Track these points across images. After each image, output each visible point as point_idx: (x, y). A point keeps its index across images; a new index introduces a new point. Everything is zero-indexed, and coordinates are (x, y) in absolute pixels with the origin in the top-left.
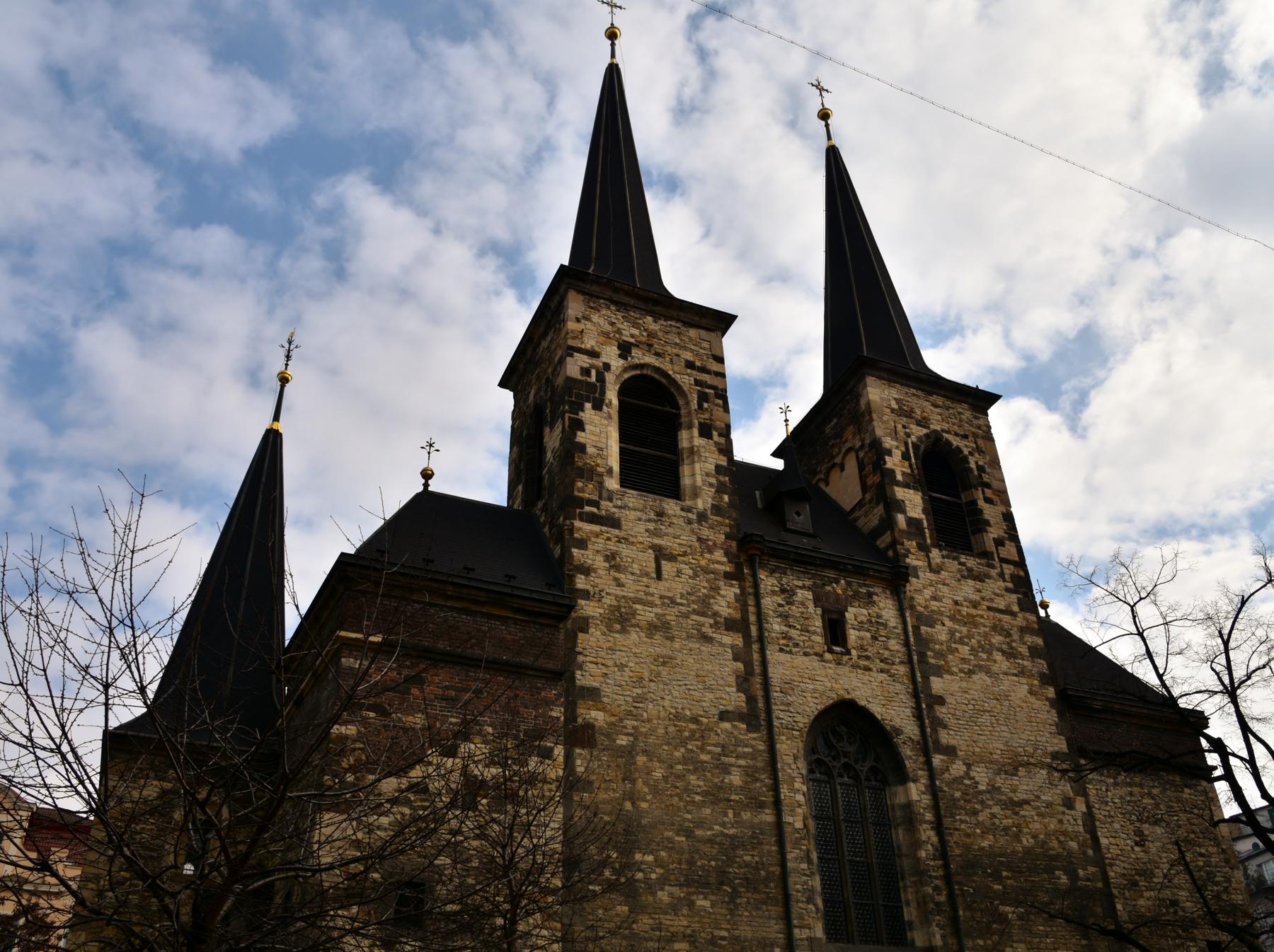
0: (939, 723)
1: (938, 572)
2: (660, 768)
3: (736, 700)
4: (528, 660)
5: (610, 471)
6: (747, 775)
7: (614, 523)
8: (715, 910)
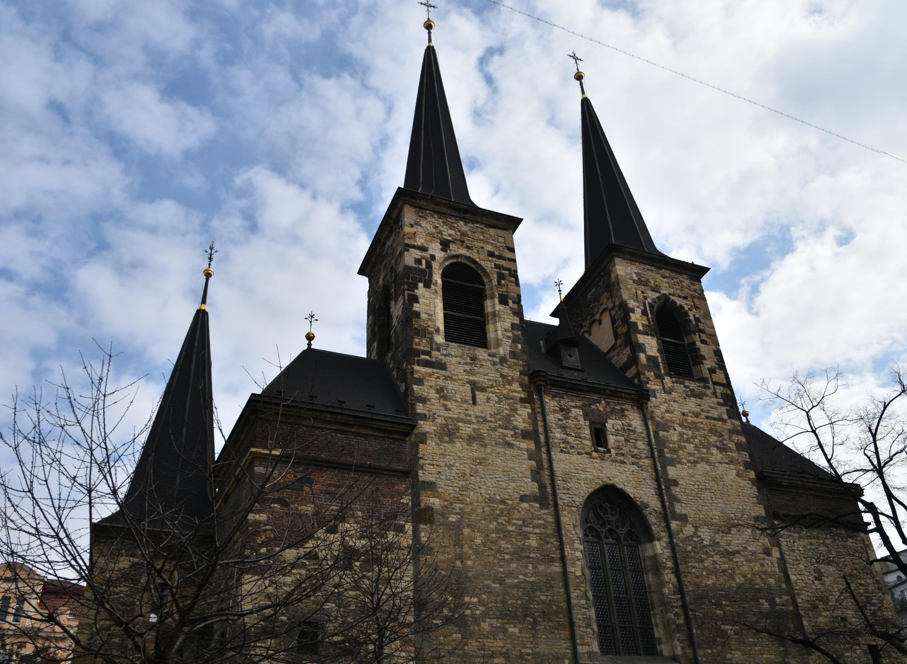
0: (674, 499)
1: (670, 393)
2: (480, 536)
3: (531, 487)
4: (384, 464)
5: (438, 330)
6: (541, 539)
7: (442, 366)
8: (522, 634)
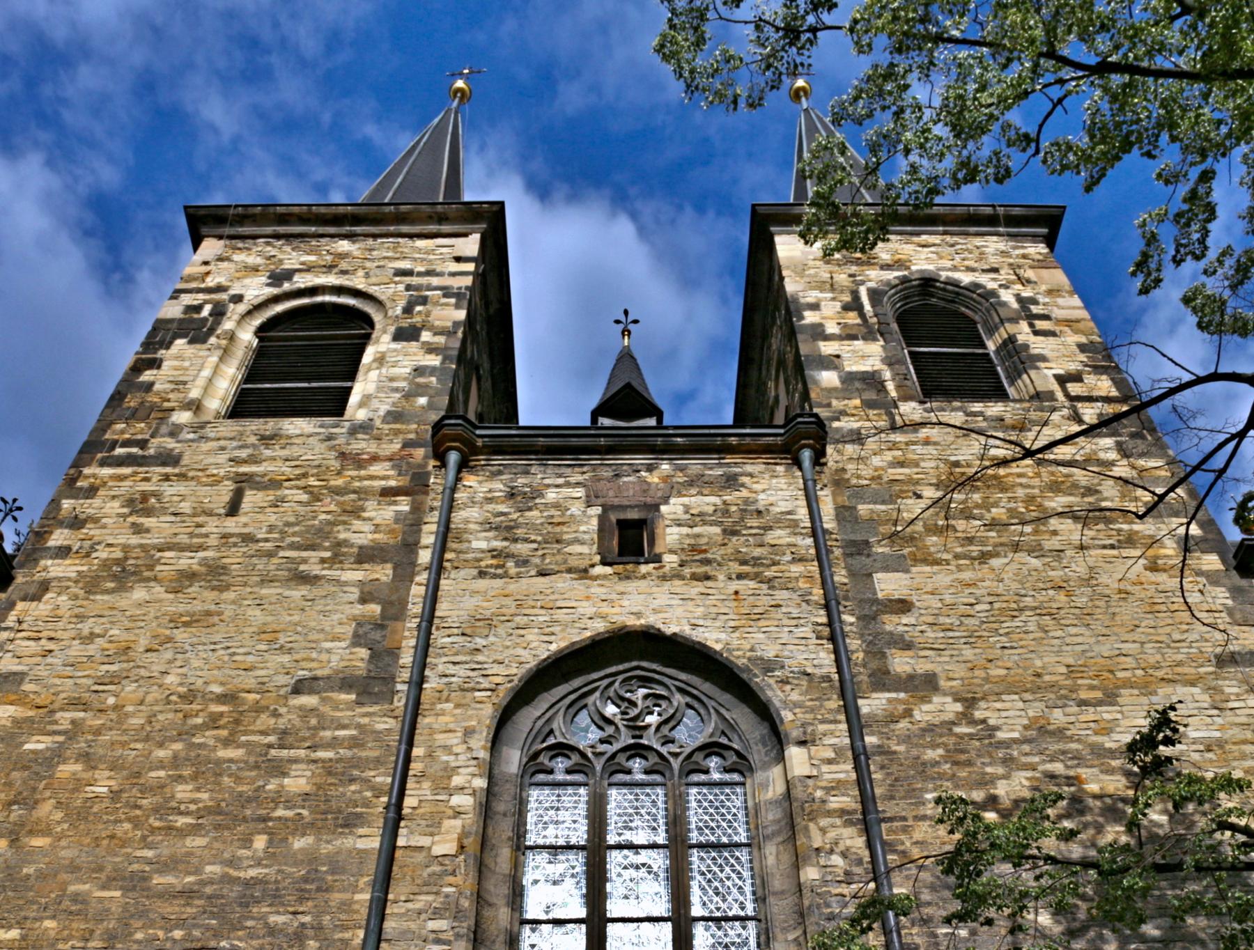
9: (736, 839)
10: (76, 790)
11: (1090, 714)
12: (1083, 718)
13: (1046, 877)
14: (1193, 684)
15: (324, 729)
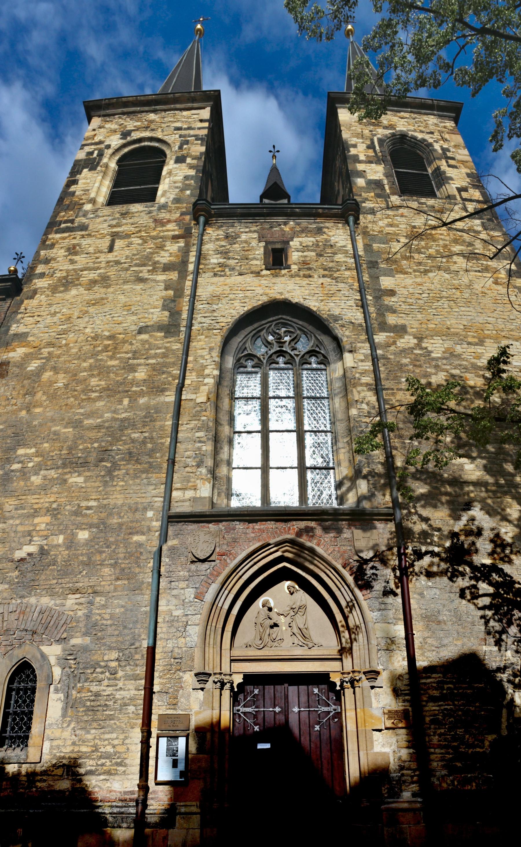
8: (88, 484)
9: (323, 395)
10: (50, 386)
11: (472, 349)
12: (469, 350)
13: (451, 419)
14: (517, 341)
15: (151, 349)
